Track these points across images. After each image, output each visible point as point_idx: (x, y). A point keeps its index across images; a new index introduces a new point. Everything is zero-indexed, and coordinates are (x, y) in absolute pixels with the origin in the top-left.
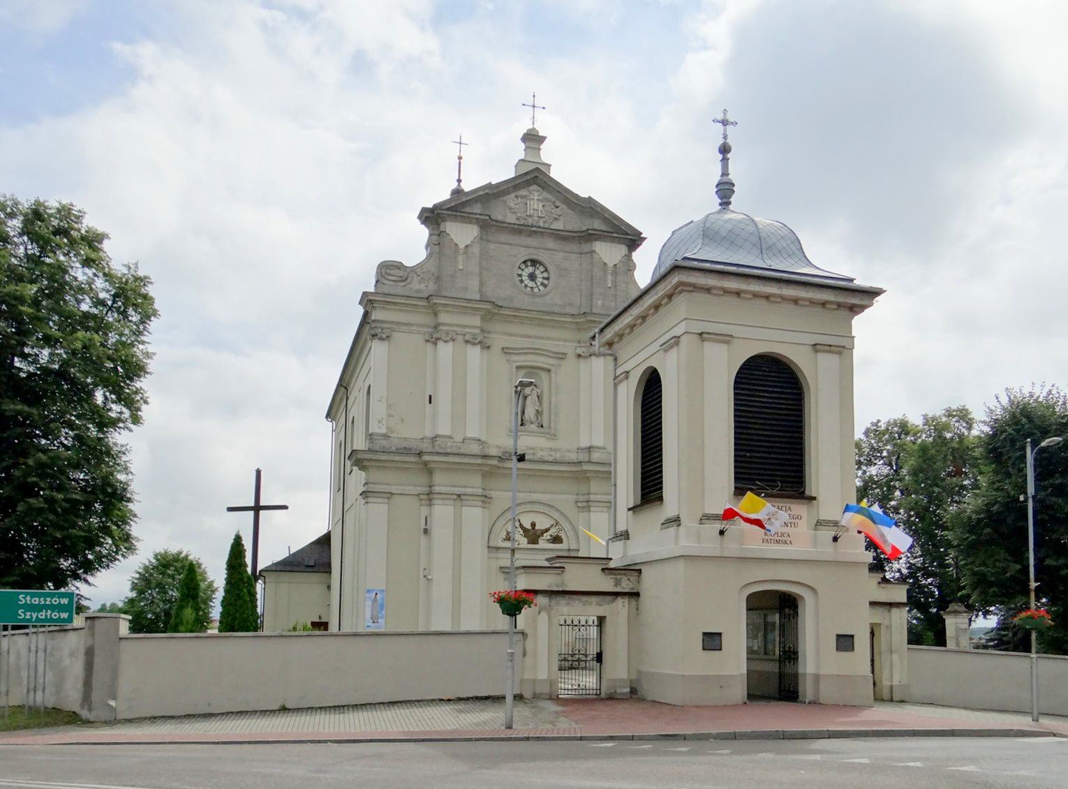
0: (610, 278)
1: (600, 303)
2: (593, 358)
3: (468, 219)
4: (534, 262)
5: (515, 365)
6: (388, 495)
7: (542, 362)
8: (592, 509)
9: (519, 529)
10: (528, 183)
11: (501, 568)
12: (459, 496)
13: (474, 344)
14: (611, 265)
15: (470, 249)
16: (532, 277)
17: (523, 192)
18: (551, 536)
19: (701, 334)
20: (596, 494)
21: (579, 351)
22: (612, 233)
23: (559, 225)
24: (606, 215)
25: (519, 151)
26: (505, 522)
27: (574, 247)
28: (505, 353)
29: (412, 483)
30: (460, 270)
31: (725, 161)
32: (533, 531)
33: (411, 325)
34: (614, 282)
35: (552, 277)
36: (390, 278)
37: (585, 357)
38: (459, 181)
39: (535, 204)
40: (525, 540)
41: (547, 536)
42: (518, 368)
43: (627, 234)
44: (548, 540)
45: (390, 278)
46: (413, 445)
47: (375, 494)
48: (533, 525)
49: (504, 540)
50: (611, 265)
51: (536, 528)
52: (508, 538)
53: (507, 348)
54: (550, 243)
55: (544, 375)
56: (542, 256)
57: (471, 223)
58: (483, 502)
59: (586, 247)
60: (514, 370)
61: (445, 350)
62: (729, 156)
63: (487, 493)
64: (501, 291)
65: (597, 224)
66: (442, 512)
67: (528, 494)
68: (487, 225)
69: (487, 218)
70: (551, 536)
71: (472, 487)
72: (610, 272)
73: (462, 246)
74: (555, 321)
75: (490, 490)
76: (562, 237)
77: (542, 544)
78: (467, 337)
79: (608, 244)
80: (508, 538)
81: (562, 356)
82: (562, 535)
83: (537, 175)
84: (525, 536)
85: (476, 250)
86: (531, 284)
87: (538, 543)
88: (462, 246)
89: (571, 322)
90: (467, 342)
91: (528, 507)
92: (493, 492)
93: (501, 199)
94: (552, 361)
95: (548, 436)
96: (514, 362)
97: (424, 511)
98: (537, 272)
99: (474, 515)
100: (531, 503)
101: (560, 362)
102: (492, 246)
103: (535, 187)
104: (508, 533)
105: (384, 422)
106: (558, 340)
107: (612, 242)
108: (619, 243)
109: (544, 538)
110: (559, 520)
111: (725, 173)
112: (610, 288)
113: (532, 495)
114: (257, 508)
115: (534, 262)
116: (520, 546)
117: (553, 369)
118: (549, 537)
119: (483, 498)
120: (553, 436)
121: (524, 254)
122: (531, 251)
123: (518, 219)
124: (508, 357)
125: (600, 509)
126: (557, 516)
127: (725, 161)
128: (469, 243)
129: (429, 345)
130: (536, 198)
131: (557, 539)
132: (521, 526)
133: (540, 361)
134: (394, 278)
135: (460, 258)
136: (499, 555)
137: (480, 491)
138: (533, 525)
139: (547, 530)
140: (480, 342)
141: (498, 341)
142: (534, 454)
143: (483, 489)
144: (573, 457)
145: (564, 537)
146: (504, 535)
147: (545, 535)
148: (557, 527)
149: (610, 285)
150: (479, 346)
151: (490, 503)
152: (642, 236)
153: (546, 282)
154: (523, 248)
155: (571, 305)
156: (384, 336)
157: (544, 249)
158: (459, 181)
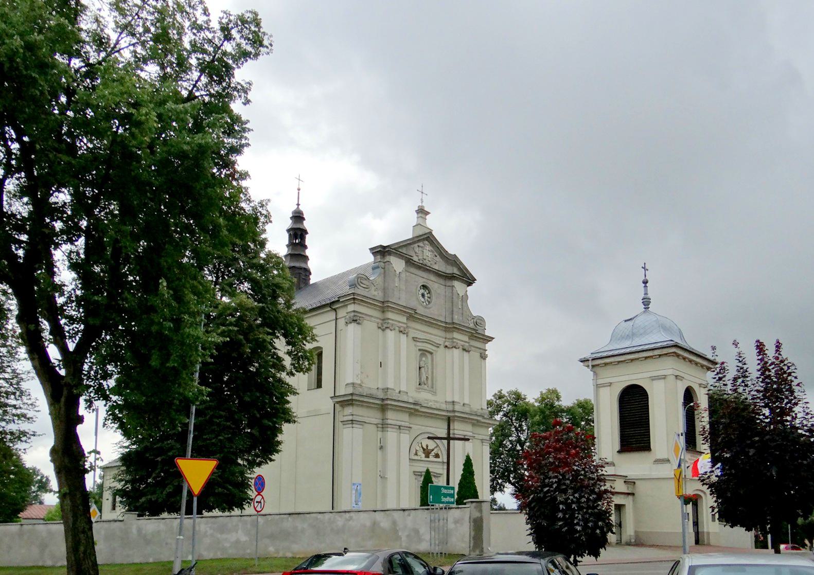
0: (460, 303)
1: (456, 317)
2: (454, 349)
3: (401, 256)
4: (424, 287)
10: (424, 239)
11: (414, 472)
12: (399, 426)
14: (461, 296)
16: (423, 295)
17: (421, 244)
19: (676, 376)
21: (447, 344)
23: (436, 267)
25: (414, 219)
27: (442, 281)
29: (372, 416)
31: (646, 286)
33: (372, 316)
35: (434, 298)
36: (362, 285)
37: (449, 348)
38: (298, 205)
39: (426, 254)
40: (423, 455)
42: (420, 350)
43: (469, 279)
45: (362, 285)
46: (374, 392)
47: (358, 423)
48: (427, 446)
50: (461, 296)
52: (416, 454)
53: (417, 338)
54: (433, 277)
55: (429, 356)
56: (430, 284)
59: (449, 283)
61: (391, 335)
62: (647, 285)
63: (411, 426)
65: (456, 271)
66: (391, 435)
68: (409, 262)
73: (398, 273)
76: (438, 274)
77: (431, 458)
78: (402, 329)
81: (438, 346)
82: (440, 453)
86: (423, 300)
88: (398, 273)
94: (434, 348)
97: (380, 434)
98: (425, 293)
103: (426, 242)
111: (646, 294)
114: (449, 438)
115: (424, 287)
121: (422, 282)
122: (425, 280)
123: (419, 260)
124: (415, 343)
127: (646, 286)
128: (401, 271)
129: (380, 330)
131: (437, 456)
134: (364, 286)
138: (427, 446)
139: (433, 450)
141: (412, 333)
142: (428, 403)
144: (444, 406)
153: (429, 300)
154: (421, 278)
155: (441, 315)
156: (392, 328)
158: (298, 205)
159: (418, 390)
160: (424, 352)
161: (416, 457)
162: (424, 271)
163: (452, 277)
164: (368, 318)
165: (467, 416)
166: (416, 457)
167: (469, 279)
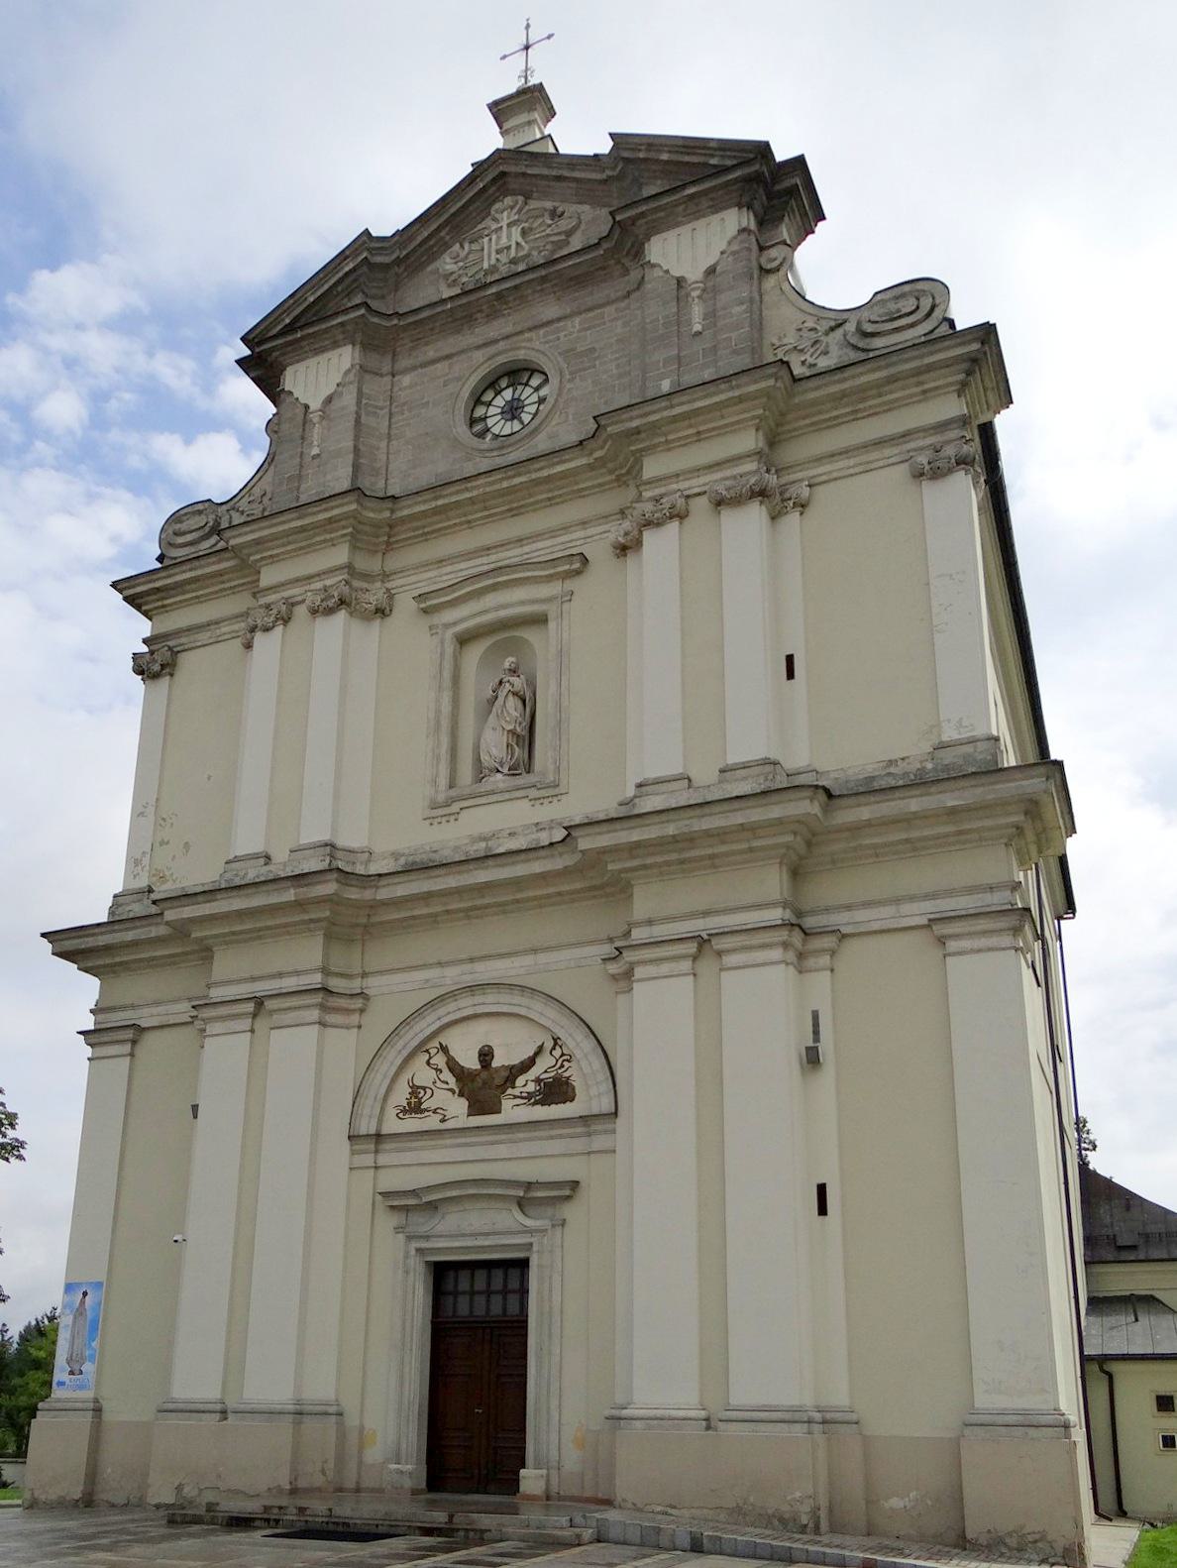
5: (449, 633)
6: (129, 1034)
7: (523, 603)
8: (639, 972)
9: (447, 1075)
11: (386, 1195)
12: (259, 1002)
13: (330, 611)
15: (336, 404)
18: (538, 1081)
20: (650, 922)
22: (684, 186)
24: (665, 157)
26: (399, 1061)
28: (425, 611)
30: (314, 457)
32: (484, 1074)
34: (711, 316)
36: (180, 540)
40: (462, 1105)
41: (526, 1083)
42: (464, 640)
43: (727, 170)
44: (530, 1096)
45: (180, 540)
48: (486, 1055)
49: (404, 1111)
51: (495, 1064)
52: (414, 1108)
57: (336, 345)
58: (323, 1007)
60: (449, 649)
64: (404, 468)
67: (468, 967)
69: (363, 311)
70: (538, 1081)
71: (297, 973)
72: (695, 294)
73: (315, 404)
74: (549, 479)
75: (364, 975)
77: (512, 1110)
79: (685, 230)
80: (414, 1108)
82: (573, 1073)
83: (501, 168)
84: (461, 1095)
85: (349, 399)
87: (499, 1112)
88: (315, 404)
89: (591, 467)
90: (314, 612)
91: (466, 1005)
92: (371, 981)
93: (429, 269)
95: (533, 793)
96: (447, 626)
99: (296, 1046)
100: (472, 989)
101: (569, 585)
102: (406, 380)
104: (415, 1090)
105: (146, 861)
106: (566, 529)
107: (698, 215)
108: (716, 208)
109: (516, 1092)
110: (560, 1033)
112: (698, 334)
113: (479, 967)
116: (450, 1125)
117: (552, 610)
118: (531, 1087)
119: (318, 998)
120: (553, 790)
125: (665, 968)
126: (550, 1015)
128: (330, 389)
130: (504, 223)
131: (556, 1090)
132: (453, 1066)
133: (514, 601)
134: (189, 538)
135: (316, 433)
136: (383, 1159)
137: (316, 979)
138: (486, 1055)
140: (342, 602)
143: (325, 971)
145: (577, 1083)
146: (401, 1095)
147: (520, 1081)
148: (557, 1052)
149: (697, 327)
150: (342, 615)
151: (362, 1011)
152: (781, 154)
157: (530, 329)
159: (443, 808)
160: (507, 633)
161: (412, 1124)
162: (493, 315)
163: (624, 244)
164: (204, 637)
165: (671, 830)
166: (412, 1124)
167: (727, 170)
